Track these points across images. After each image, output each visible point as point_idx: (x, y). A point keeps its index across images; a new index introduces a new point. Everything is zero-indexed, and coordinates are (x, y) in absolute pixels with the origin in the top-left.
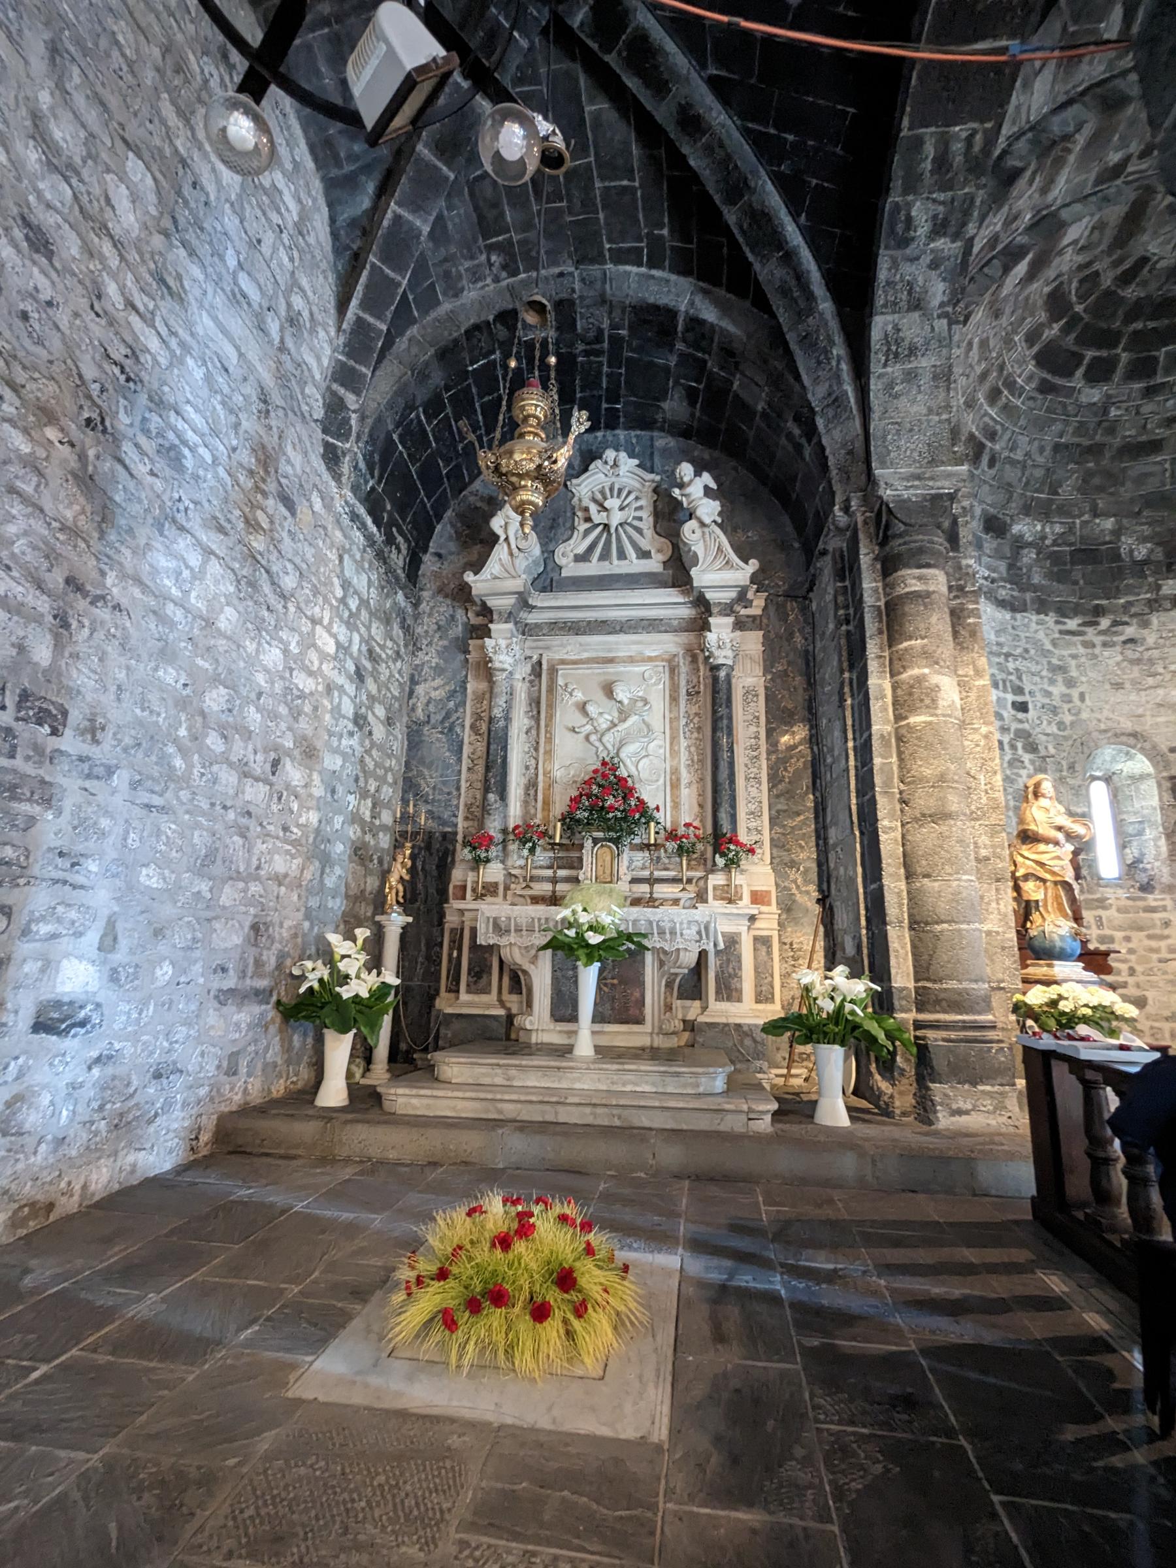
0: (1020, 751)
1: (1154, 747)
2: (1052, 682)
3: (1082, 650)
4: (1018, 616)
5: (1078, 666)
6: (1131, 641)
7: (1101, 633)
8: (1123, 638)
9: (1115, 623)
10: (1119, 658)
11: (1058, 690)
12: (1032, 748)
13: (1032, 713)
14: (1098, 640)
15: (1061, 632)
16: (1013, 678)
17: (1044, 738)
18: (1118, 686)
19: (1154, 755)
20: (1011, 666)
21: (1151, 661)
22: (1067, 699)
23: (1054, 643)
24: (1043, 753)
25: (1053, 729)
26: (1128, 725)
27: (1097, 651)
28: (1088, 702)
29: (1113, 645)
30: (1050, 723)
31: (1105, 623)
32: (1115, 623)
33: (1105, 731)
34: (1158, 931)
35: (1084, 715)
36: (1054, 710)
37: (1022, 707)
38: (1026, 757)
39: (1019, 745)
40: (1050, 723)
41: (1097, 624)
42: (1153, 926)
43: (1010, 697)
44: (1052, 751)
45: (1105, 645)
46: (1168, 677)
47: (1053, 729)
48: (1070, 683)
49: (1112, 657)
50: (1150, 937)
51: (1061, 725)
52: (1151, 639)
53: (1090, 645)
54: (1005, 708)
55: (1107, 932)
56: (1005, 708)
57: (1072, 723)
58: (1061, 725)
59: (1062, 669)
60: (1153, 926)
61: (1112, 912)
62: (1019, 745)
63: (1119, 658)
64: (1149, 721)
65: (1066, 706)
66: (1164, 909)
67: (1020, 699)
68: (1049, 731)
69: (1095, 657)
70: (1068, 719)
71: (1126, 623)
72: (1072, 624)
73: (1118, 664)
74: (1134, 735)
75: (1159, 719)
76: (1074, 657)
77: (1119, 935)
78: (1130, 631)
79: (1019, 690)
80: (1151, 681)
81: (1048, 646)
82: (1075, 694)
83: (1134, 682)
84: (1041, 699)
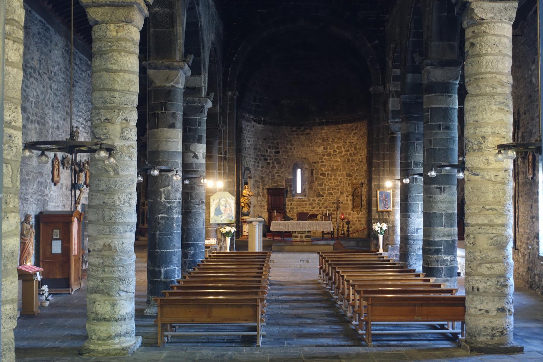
0: (275, 164)
1: (309, 162)
2: (287, 145)
3: (296, 136)
4: (280, 127)
5: (294, 140)
6: (308, 134)
7: (302, 131)
8: (306, 133)
9: (305, 129)
10: (304, 138)
11: (288, 147)
12: (279, 163)
13: (280, 154)
14: (300, 133)
15: (291, 131)
16: (276, 145)
17: (283, 160)
18: (303, 146)
19: (310, 164)
20: (275, 142)
21: (311, 140)
22: (291, 149)
23: (289, 134)
24: (282, 163)
25: (286, 157)
26: (304, 156)
27: (300, 136)
28: (296, 150)
29: (303, 135)
30: (285, 155)
31: (302, 128)
32: (305, 129)
33: (299, 157)
34: (304, 206)
35: (294, 153)
36: (287, 152)
37: (278, 152)
38: (277, 166)
39: (275, 163)
40: (285, 155)
41: (301, 129)
42: (303, 205)
43: (274, 150)
44: (285, 163)
45: (302, 134)
46: (315, 144)
47: (286, 157)
48: (292, 145)
49: (303, 138)
50: (302, 208)
51: (288, 156)
52: (312, 134)
53: (298, 134)
54: (272, 153)
55: (293, 206)
56: (272, 153)
57: (291, 156)
58: (288, 156)
59: (291, 141)
60: (303, 205)
61: (295, 202)
62: (275, 163)
63: (304, 138)
64: (309, 155)
65: (290, 151)
66: (306, 201)
67: (277, 150)
68: (285, 157)
69: (299, 137)
70: (290, 154)
71: (307, 129)
72: (294, 129)
73: (304, 140)
74: (305, 158)
75: (312, 155)
76: (293, 138)
77: (295, 207)
78: (308, 131)
79: (278, 148)
80: (311, 145)
81: (287, 135)
82: (293, 148)
83: (307, 145)
84: (283, 149)
